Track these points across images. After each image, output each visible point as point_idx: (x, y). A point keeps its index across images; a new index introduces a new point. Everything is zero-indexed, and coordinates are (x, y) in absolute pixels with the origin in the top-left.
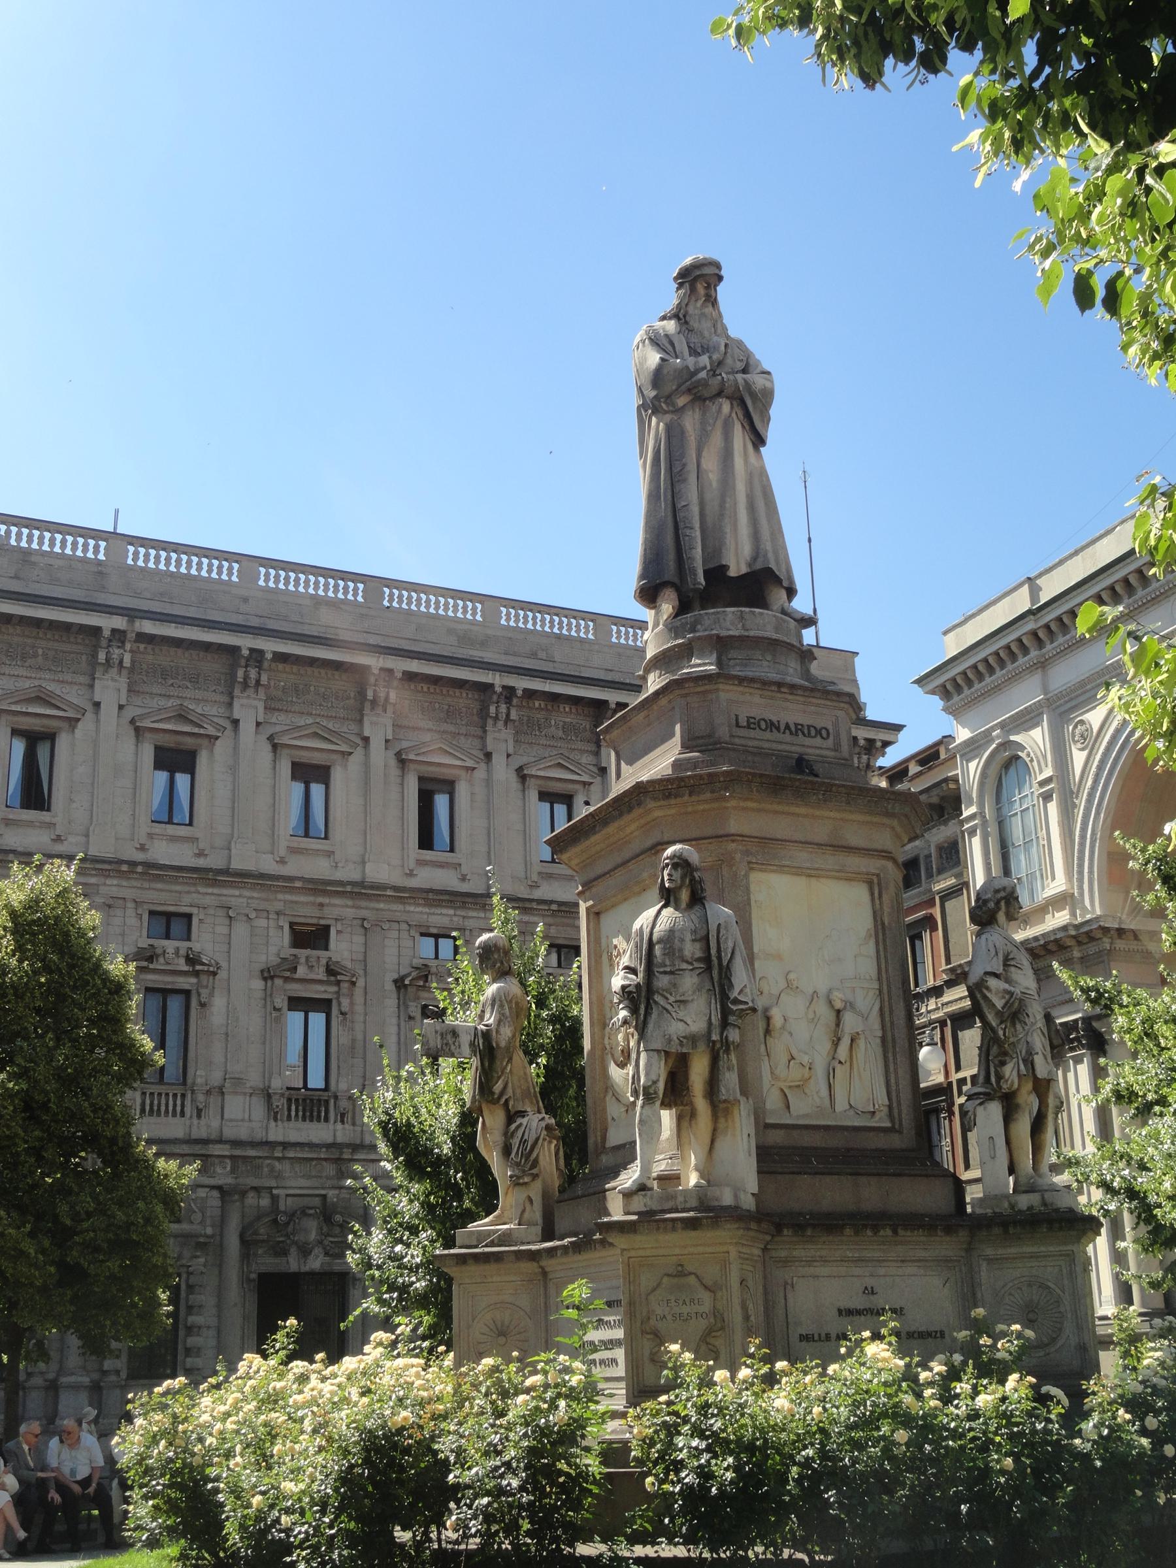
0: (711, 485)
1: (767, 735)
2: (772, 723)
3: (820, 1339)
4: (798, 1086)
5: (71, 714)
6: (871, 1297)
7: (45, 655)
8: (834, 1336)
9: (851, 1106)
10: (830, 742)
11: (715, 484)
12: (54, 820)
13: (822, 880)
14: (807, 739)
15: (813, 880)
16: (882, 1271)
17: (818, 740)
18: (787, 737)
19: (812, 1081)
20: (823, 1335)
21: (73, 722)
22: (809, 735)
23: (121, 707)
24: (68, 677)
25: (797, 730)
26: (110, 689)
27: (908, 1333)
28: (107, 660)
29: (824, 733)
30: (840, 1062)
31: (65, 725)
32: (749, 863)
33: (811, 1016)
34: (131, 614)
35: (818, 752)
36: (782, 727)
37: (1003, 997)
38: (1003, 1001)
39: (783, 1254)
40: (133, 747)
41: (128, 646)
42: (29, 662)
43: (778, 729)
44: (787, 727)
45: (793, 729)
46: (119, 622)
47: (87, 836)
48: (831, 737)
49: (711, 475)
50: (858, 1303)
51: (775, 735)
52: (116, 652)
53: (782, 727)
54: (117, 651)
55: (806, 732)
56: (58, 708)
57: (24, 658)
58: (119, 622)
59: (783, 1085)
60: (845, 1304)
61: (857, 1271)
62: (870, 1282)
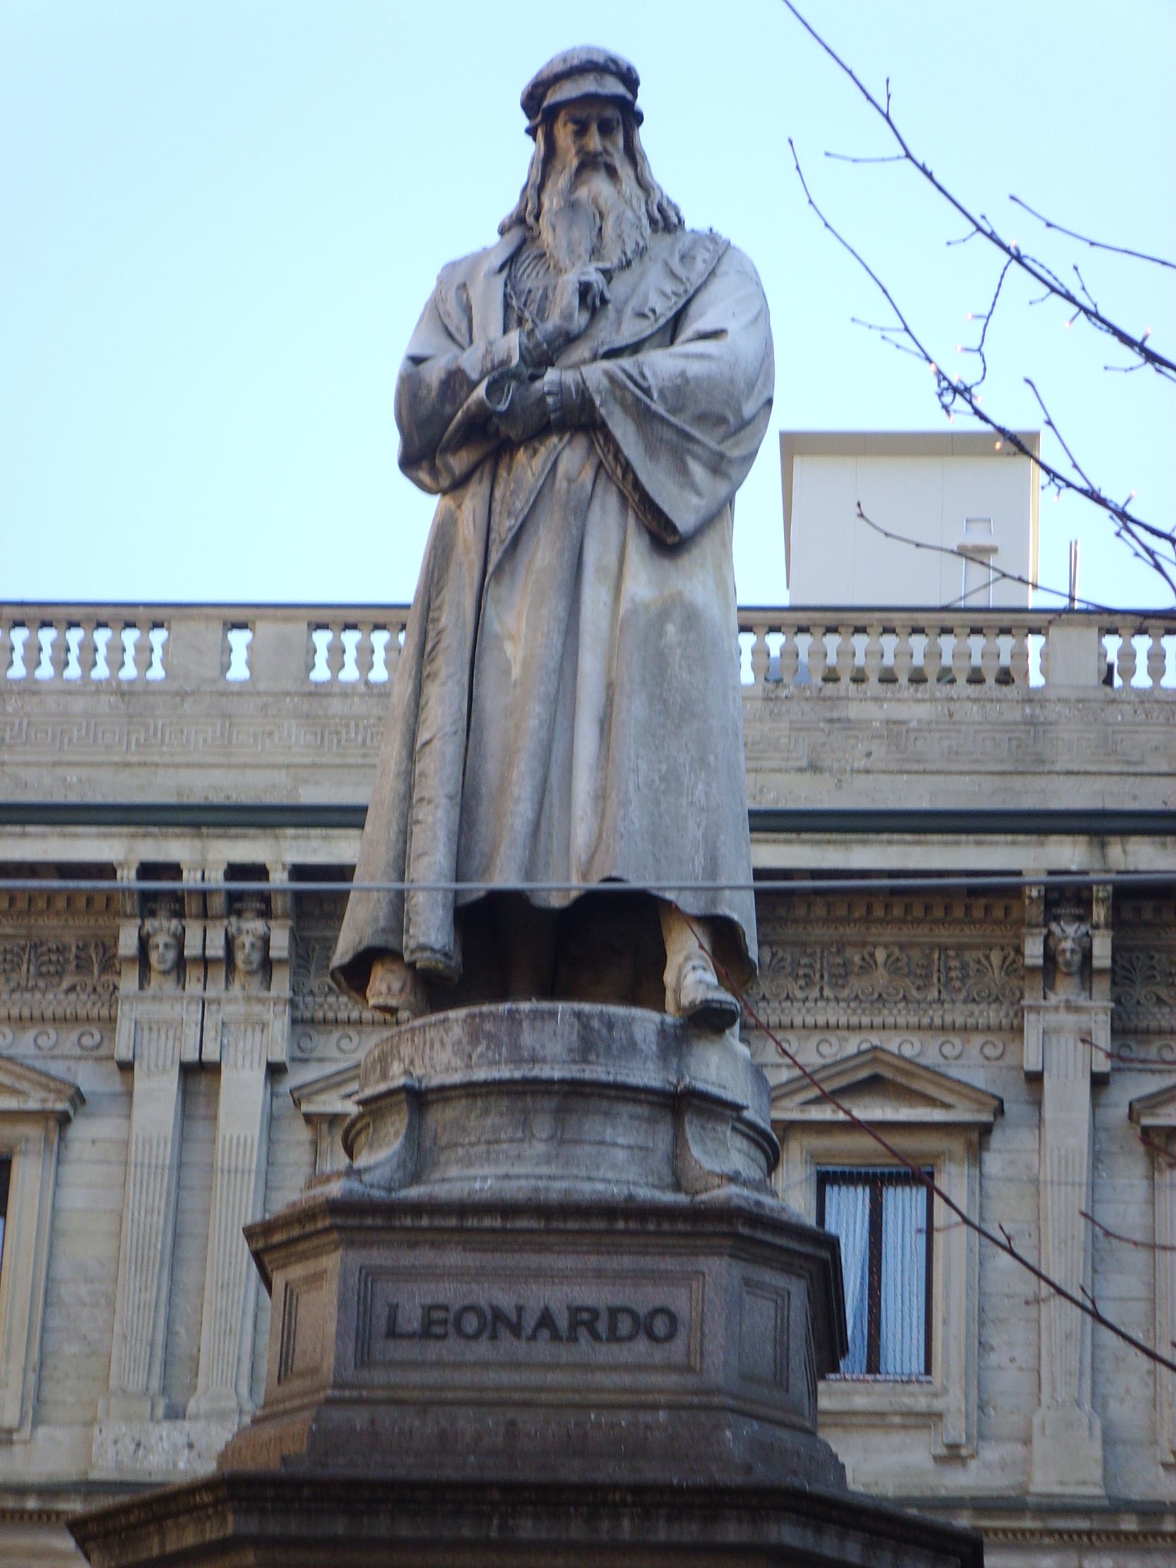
0: (507, 672)
1: (482, 1349)
2: (498, 1314)
5: (962, 1113)
7: (893, 966)
10: (676, 1350)
11: (516, 671)
12: (939, 1404)
17: (642, 1346)
18: (543, 1349)
21: (977, 1137)
23: (1099, 1082)
24: (958, 1014)
25: (574, 1325)
26: (1066, 1035)
28: (1049, 955)
29: (660, 1326)
31: (956, 1145)
34: (1098, 825)
35: (627, 1379)
36: (530, 1322)
40: (1140, 1187)
41: (1099, 913)
42: (856, 985)
43: (516, 1330)
44: (546, 1320)
45: (562, 1322)
46: (1067, 854)
47: (1027, 1441)
48: (682, 1333)
49: (509, 648)
51: (508, 1346)
52: (1068, 933)
53: (530, 1322)
54: (1071, 930)
55: (602, 1327)
56: (932, 1102)
57: (841, 977)
58: (1067, 854)
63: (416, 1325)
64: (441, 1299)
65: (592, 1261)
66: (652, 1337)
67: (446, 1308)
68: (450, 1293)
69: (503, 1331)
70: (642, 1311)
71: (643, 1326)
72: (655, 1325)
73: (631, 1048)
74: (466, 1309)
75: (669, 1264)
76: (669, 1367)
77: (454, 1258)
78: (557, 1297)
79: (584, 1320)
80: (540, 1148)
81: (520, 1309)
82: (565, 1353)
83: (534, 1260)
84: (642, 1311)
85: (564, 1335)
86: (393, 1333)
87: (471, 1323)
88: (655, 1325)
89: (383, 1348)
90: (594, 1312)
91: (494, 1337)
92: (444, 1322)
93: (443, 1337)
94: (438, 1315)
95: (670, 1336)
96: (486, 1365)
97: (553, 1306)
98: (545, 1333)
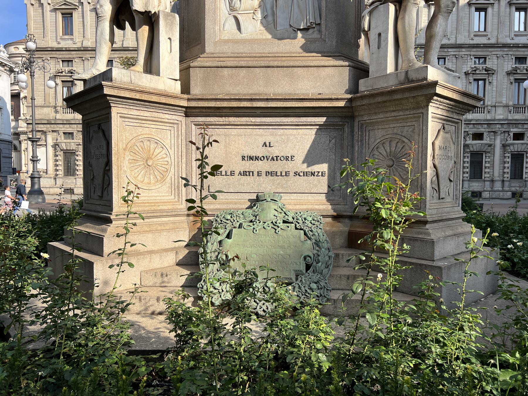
6: (269, 149)
8: (237, 173)
9: (291, 26)
59: (235, 13)
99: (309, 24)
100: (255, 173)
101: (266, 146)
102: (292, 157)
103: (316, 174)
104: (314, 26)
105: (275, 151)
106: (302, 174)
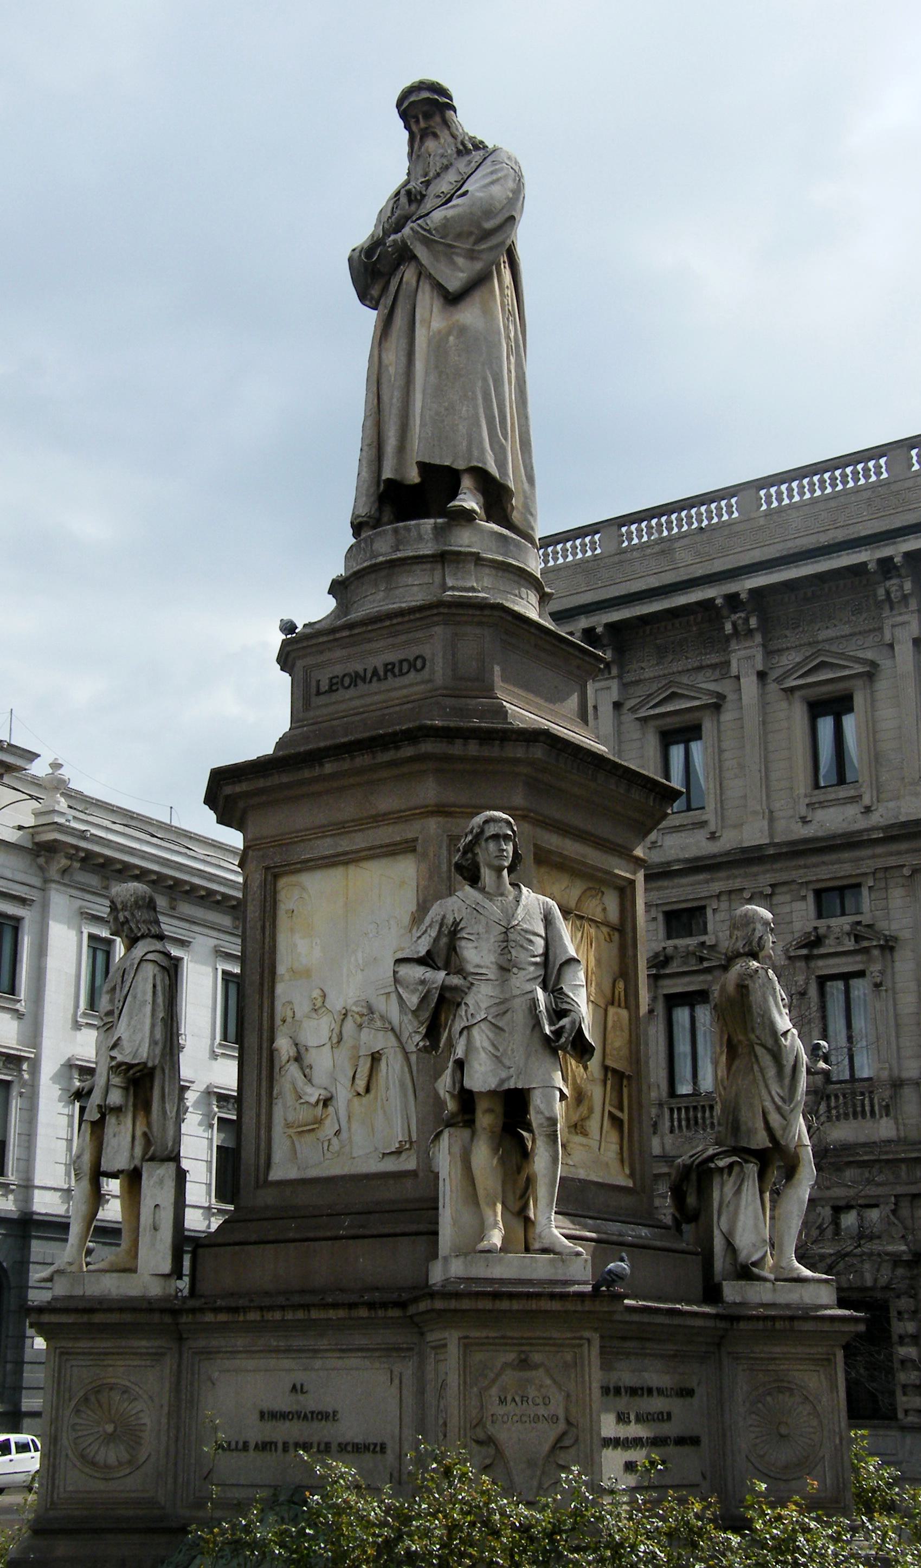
1: (352, 692)
2: (357, 673)
3: (237, 1449)
4: (313, 1130)
6: (301, 1397)
8: (252, 1445)
10: (426, 674)
13: (361, 864)
14: (397, 680)
15: (352, 869)
16: (318, 1363)
17: (412, 674)
18: (375, 685)
19: (328, 1122)
20: (240, 1445)
22: (402, 674)
27: (340, 1444)
29: (419, 664)
30: (359, 1094)
32: (267, 868)
33: (335, 1041)
37: (416, 990)
38: (417, 994)
39: (201, 1343)
43: (364, 679)
44: (375, 672)
45: (382, 673)
50: (284, 1403)
51: (362, 688)
60: (268, 1405)
61: (286, 1363)
62: (299, 1377)
63: (327, 688)
64: (336, 674)
65: (390, 641)
66: (418, 671)
67: (338, 677)
68: (338, 670)
69: (359, 681)
70: (411, 658)
71: (412, 665)
72: (416, 664)
73: (420, 538)
74: (344, 676)
75: (420, 634)
76: (423, 682)
77: (339, 653)
78: (377, 661)
79: (389, 668)
80: (382, 594)
81: (365, 670)
82: (384, 686)
83: (368, 647)
84: (411, 658)
85: (382, 677)
86: (318, 693)
87: (347, 681)
88: (416, 664)
89: (322, 700)
90: (393, 664)
91: (356, 685)
92: (337, 683)
93: (337, 690)
94: (334, 681)
95: (423, 667)
96: (351, 699)
97: (377, 665)
98: (375, 679)
99: (397, 1145)
100: (280, 1446)
101: (296, 1391)
102: (335, 1413)
103: (372, 1447)
104: (407, 1146)
105: (310, 1403)
106: (349, 1448)
